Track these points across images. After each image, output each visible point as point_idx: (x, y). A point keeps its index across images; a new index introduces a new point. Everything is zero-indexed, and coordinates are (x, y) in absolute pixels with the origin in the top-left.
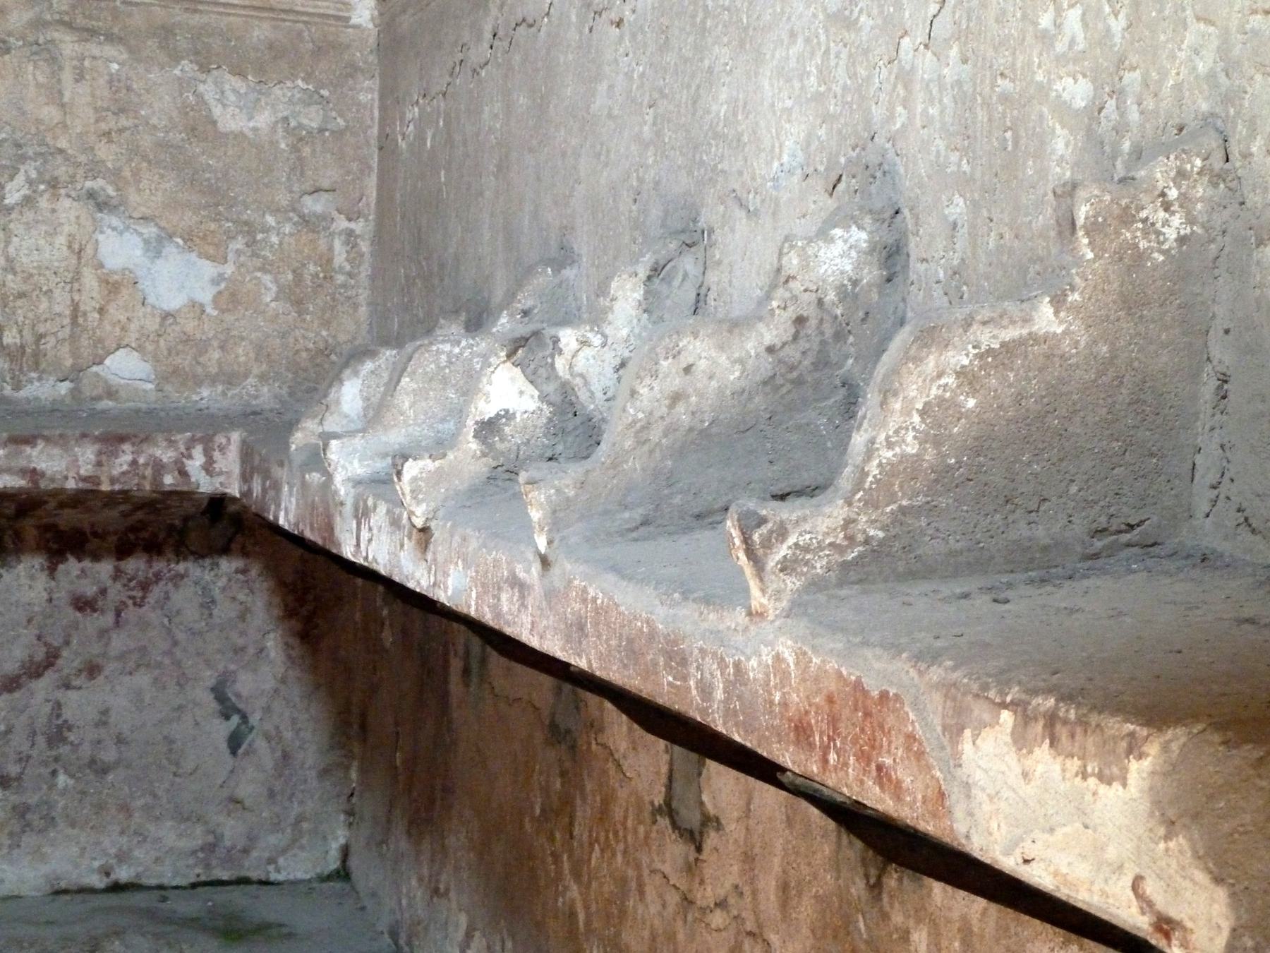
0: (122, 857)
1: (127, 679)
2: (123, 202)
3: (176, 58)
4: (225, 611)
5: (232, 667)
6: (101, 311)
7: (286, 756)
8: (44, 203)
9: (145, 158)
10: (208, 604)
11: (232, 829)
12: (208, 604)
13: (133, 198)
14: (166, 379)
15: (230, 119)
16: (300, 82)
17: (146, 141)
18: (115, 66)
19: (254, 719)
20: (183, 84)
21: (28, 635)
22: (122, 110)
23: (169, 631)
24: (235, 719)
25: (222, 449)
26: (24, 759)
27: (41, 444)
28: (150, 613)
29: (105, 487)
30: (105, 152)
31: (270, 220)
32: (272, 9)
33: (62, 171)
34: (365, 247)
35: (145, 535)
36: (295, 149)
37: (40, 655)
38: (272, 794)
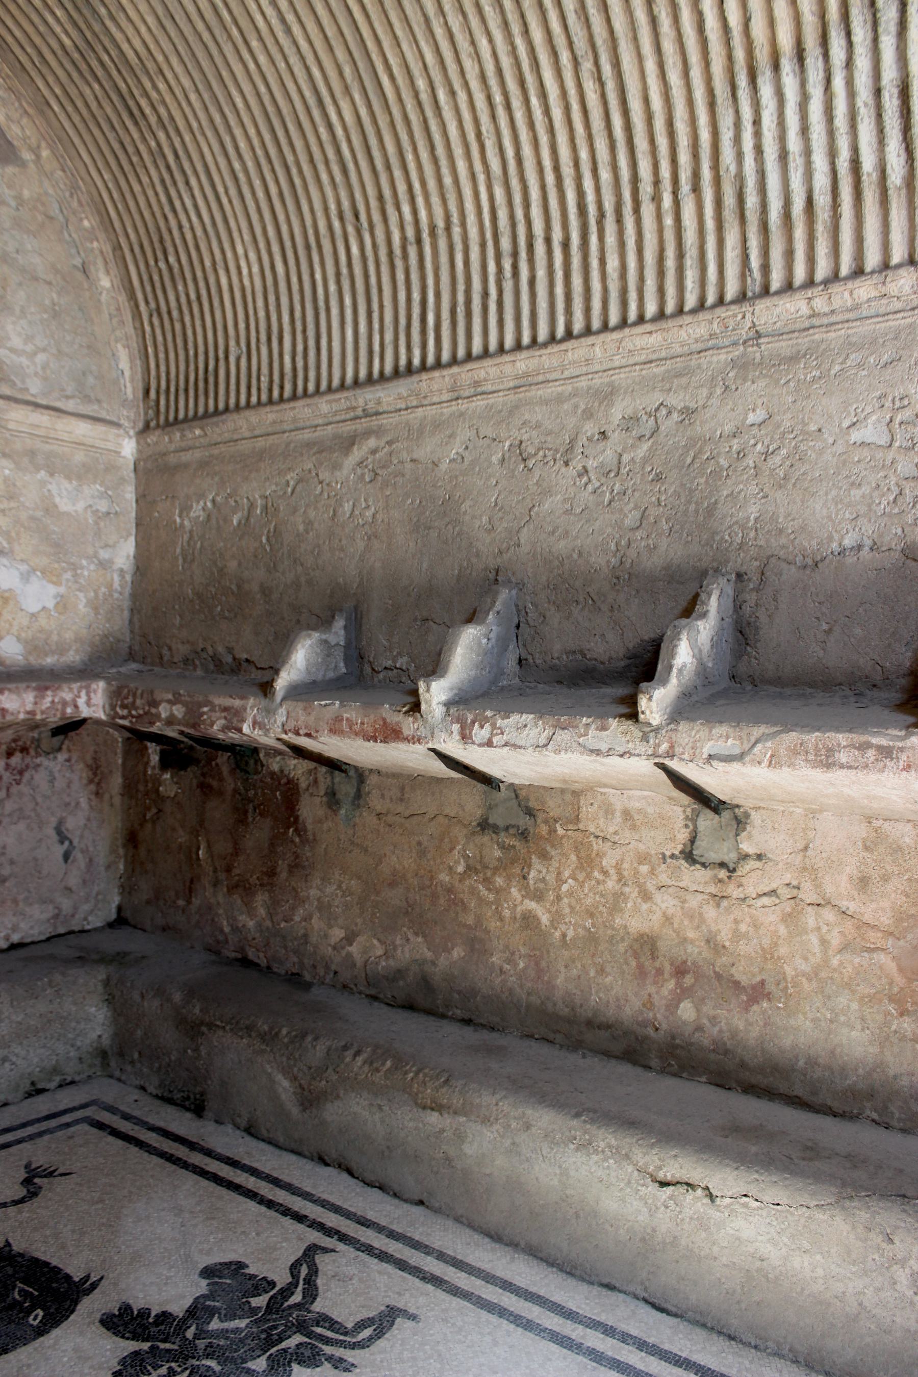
1: (13, 827)
2: (12, 551)
3: (38, 470)
4: (60, 784)
5: (64, 814)
7: (91, 860)
10: (52, 780)
11: (66, 904)
12: (52, 780)
13: (17, 548)
14: (30, 653)
15: (65, 505)
16: (98, 487)
17: (23, 516)
18: (7, 472)
19: (75, 842)
20: (43, 483)
22: (11, 498)
23: (34, 798)
24: (67, 843)
25: (95, 691)
27: (6, 693)
28: (23, 788)
31: (84, 562)
32: (84, 444)
34: (128, 578)
35: (20, 743)
36: (96, 523)
38: (84, 882)
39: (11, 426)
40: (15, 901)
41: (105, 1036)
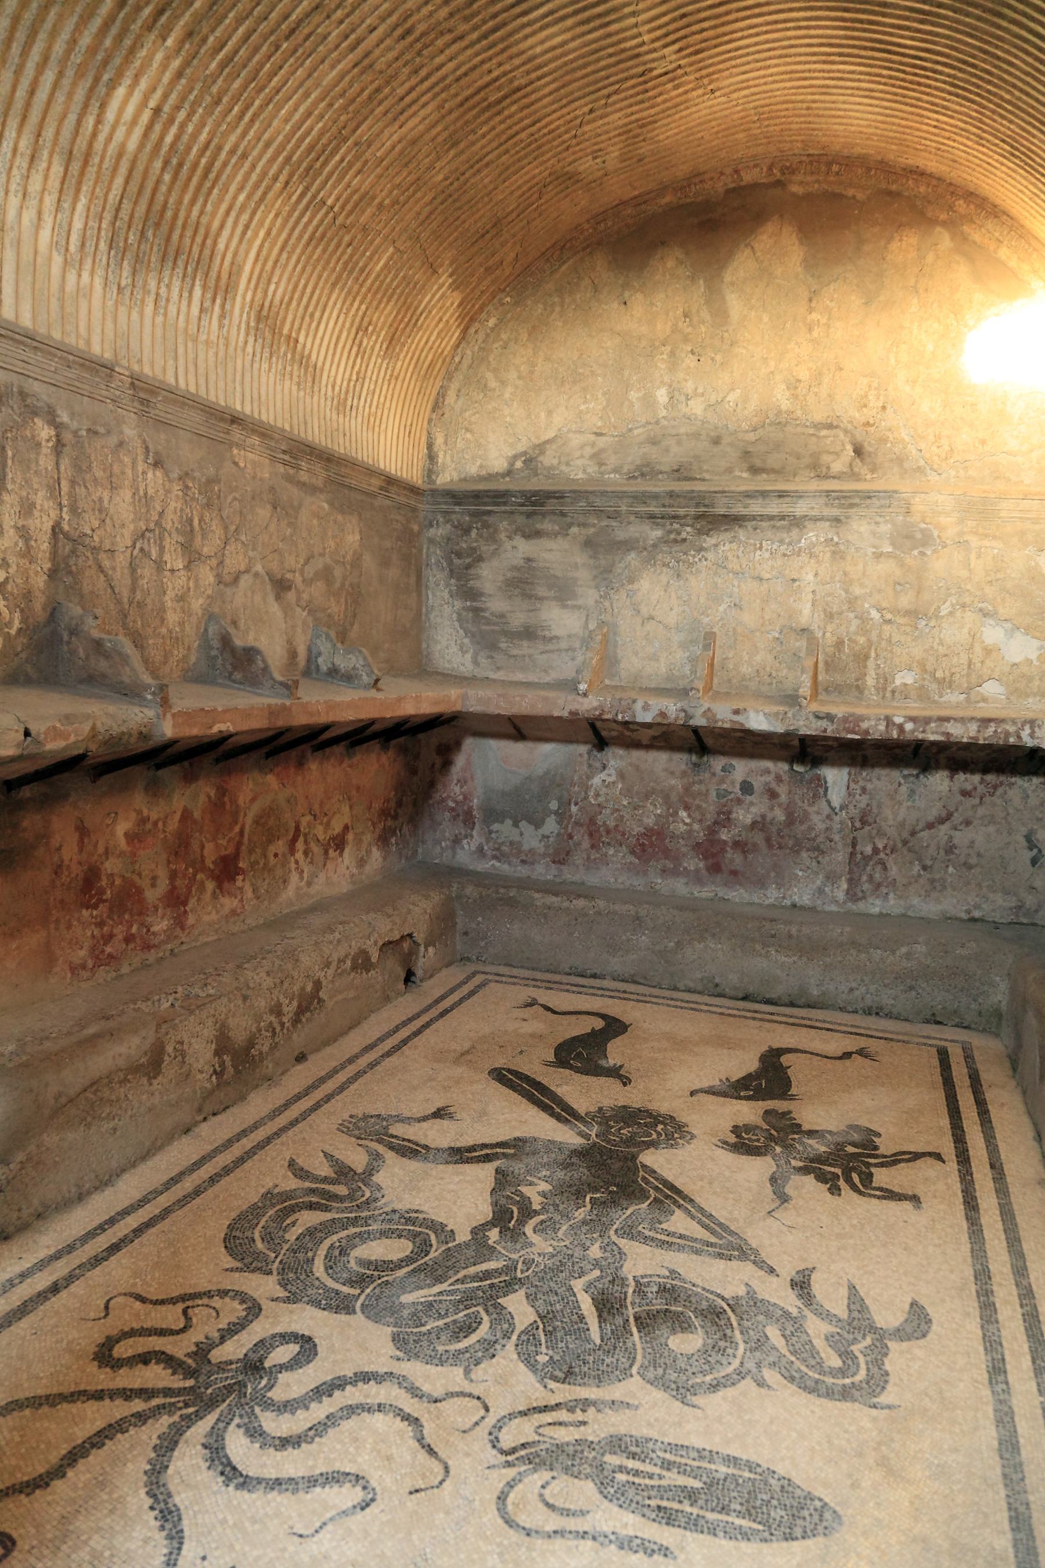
0: (977, 907)
2: (996, 613)
4: (1033, 801)
6: (982, 662)
8: (958, 614)
9: (1008, 592)
11: (1030, 901)
21: (939, 805)
24: (1035, 851)
26: (934, 859)
29: (981, 742)
30: (989, 591)
33: (968, 600)
37: (944, 814)
39: (1003, 514)
40: (979, 885)
41: (1004, 1003)
